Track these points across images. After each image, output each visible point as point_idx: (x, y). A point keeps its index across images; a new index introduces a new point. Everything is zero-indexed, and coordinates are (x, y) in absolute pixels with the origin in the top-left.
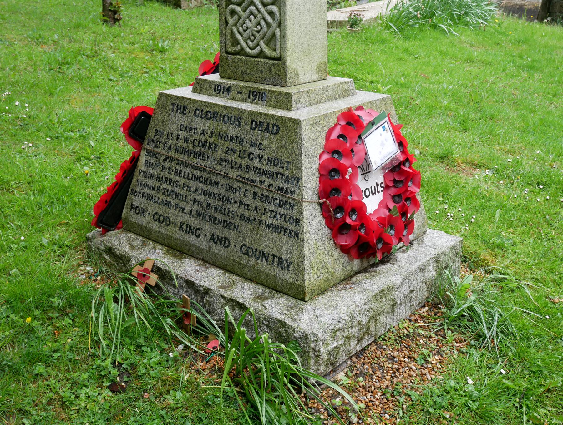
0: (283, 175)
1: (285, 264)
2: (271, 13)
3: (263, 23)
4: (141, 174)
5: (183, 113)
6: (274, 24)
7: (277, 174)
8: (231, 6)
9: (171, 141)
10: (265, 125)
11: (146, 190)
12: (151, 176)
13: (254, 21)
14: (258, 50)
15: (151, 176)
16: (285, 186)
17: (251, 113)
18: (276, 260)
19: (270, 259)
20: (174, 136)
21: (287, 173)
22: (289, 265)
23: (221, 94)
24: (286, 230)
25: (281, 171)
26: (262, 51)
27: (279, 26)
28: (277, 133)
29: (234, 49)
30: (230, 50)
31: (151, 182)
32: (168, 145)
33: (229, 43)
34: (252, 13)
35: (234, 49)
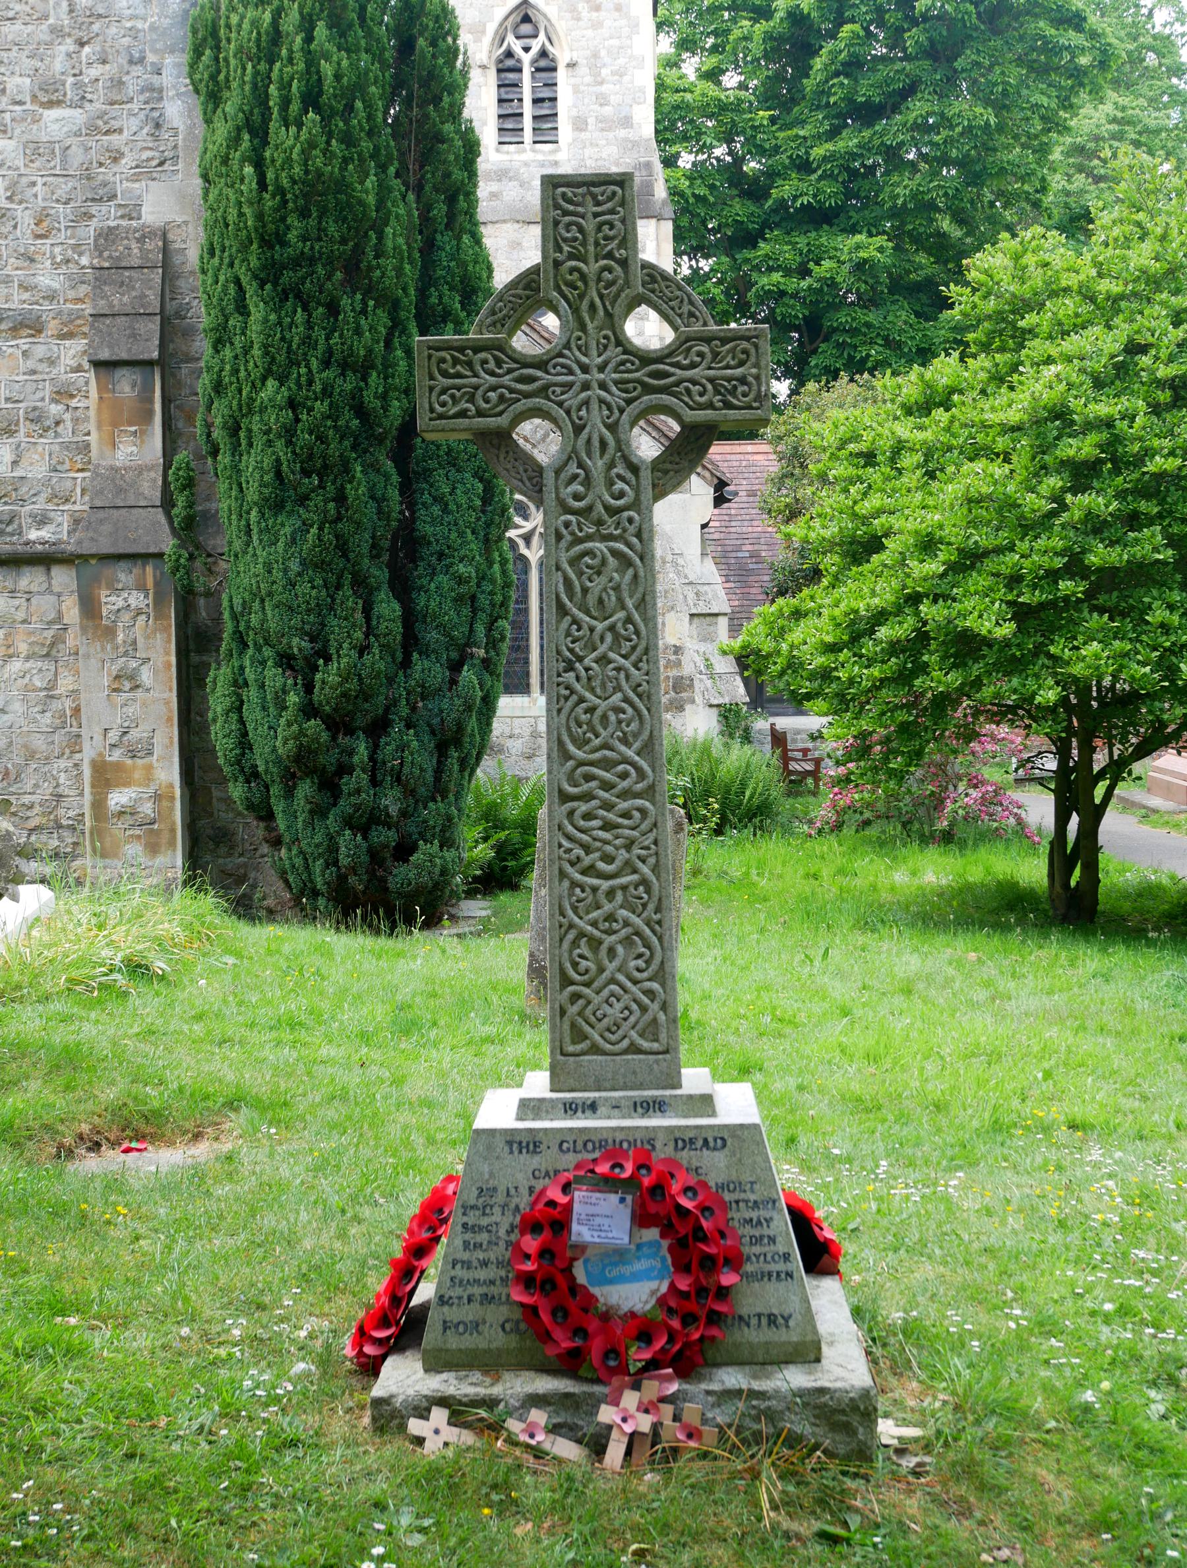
0: (747, 1201)
1: (780, 1320)
2: (650, 993)
3: (634, 1007)
4: (459, 1266)
5: (535, 1152)
6: (655, 1007)
7: (737, 1202)
8: (571, 988)
9: (515, 1200)
10: (700, 1143)
11: (477, 1291)
12: (485, 1264)
13: (618, 1006)
14: (626, 1043)
15: (485, 1264)
16: (754, 1215)
17: (669, 1130)
18: (764, 1321)
19: (754, 1321)
20: (521, 1189)
21: (752, 1197)
22: (786, 1319)
23: (579, 1113)
24: (770, 1274)
25: (743, 1196)
26: (632, 1044)
27: (664, 1007)
28: (724, 1145)
29: (579, 1048)
30: (571, 1049)
31: (482, 1274)
32: (513, 1206)
33: (567, 1039)
34: (612, 995)
35: (579, 1048)
